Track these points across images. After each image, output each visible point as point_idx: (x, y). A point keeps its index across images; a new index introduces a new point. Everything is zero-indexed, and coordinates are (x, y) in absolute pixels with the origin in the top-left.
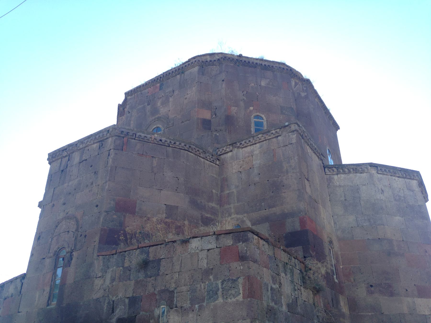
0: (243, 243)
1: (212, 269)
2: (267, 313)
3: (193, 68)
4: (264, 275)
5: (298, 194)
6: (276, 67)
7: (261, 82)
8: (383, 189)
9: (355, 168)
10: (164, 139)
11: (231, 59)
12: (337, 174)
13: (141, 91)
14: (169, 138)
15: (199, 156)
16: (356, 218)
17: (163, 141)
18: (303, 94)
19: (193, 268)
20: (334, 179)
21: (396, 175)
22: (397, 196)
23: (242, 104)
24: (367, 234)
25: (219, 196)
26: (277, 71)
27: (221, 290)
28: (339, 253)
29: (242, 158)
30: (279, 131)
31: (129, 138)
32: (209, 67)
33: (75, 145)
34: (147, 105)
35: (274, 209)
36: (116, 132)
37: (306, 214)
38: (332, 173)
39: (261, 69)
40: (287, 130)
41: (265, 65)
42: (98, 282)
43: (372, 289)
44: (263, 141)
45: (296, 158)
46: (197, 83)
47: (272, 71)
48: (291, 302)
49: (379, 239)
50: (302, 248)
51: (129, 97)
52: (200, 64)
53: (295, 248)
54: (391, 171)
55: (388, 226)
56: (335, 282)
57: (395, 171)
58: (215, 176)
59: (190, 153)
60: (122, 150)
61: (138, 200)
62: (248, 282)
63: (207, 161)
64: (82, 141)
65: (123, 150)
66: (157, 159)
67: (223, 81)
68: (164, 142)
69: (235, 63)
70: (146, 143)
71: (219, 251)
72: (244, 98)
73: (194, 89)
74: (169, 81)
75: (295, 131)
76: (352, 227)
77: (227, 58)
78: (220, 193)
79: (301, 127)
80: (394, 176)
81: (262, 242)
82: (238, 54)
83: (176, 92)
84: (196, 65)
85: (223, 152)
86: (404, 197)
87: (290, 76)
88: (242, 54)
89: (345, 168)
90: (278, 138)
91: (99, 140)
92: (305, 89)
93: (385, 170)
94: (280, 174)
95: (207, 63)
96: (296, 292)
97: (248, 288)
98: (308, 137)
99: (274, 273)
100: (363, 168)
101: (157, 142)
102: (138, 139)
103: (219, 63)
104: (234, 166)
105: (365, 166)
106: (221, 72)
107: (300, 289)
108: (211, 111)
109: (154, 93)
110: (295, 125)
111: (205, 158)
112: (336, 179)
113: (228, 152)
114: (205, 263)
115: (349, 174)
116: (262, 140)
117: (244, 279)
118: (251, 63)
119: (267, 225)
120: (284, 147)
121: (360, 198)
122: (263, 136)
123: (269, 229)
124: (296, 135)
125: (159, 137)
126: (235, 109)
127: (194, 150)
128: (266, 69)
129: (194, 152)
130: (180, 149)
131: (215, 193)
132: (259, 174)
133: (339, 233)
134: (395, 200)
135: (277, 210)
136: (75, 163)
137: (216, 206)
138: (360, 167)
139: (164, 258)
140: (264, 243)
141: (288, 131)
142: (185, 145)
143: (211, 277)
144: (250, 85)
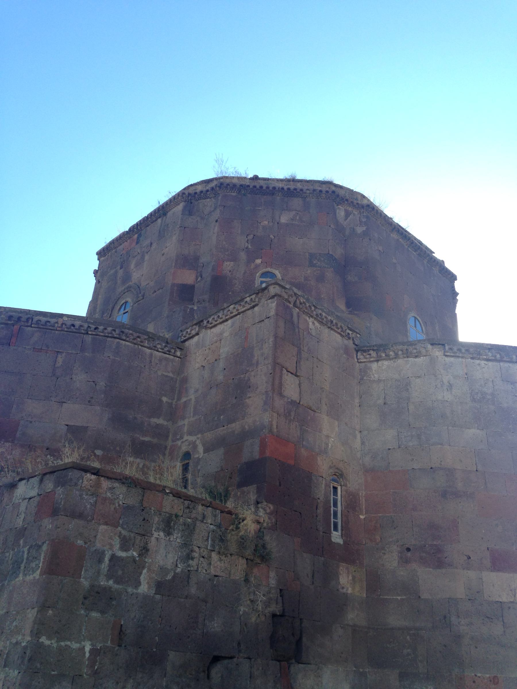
0: (61, 488)
2: (85, 598)
3: (177, 205)
4: (98, 537)
6: (307, 190)
7: (280, 217)
9: (405, 348)
12: (377, 361)
13: (115, 248)
15: (142, 346)
16: (397, 434)
17: (77, 327)
18: (360, 230)
20: (372, 369)
21: (481, 357)
22: (478, 393)
23: (243, 256)
26: (309, 196)
27: (25, 561)
35: (233, 425)
38: (368, 360)
40: (266, 295)
41: (289, 189)
43: (409, 554)
44: (236, 315)
45: (272, 339)
47: (302, 198)
48: (169, 577)
49: (431, 468)
50: (256, 488)
52: (187, 198)
54: (471, 350)
56: (330, 543)
57: (479, 350)
58: (171, 375)
59: (124, 342)
60: (9, 345)
63: (157, 353)
66: (64, 354)
69: (239, 192)
72: (248, 246)
77: (225, 185)
78: (176, 402)
80: (478, 360)
81: (105, 484)
83: (154, 246)
84: (180, 200)
85: (188, 336)
87: (335, 201)
88: (257, 175)
89: (390, 349)
90: (255, 308)
92: (364, 220)
94: (248, 369)
95: (196, 196)
96: (191, 562)
98: (307, 304)
100: (418, 348)
101: (67, 328)
103: (214, 194)
104: (198, 357)
105: (423, 345)
106: (215, 208)
107: (206, 556)
109: (130, 249)
110: (275, 286)
111: (153, 348)
115: (396, 360)
116: (234, 314)
120: (260, 323)
121: (408, 399)
124: (276, 303)
125: (70, 321)
126: (230, 265)
127: (132, 337)
128: (291, 194)
131: (166, 402)
132: (225, 369)
134: (474, 400)
135: (236, 426)
137: (165, 423)
138: (413, 347)
140: (116, 485)
141: (267, 296)
142: (115, 330)
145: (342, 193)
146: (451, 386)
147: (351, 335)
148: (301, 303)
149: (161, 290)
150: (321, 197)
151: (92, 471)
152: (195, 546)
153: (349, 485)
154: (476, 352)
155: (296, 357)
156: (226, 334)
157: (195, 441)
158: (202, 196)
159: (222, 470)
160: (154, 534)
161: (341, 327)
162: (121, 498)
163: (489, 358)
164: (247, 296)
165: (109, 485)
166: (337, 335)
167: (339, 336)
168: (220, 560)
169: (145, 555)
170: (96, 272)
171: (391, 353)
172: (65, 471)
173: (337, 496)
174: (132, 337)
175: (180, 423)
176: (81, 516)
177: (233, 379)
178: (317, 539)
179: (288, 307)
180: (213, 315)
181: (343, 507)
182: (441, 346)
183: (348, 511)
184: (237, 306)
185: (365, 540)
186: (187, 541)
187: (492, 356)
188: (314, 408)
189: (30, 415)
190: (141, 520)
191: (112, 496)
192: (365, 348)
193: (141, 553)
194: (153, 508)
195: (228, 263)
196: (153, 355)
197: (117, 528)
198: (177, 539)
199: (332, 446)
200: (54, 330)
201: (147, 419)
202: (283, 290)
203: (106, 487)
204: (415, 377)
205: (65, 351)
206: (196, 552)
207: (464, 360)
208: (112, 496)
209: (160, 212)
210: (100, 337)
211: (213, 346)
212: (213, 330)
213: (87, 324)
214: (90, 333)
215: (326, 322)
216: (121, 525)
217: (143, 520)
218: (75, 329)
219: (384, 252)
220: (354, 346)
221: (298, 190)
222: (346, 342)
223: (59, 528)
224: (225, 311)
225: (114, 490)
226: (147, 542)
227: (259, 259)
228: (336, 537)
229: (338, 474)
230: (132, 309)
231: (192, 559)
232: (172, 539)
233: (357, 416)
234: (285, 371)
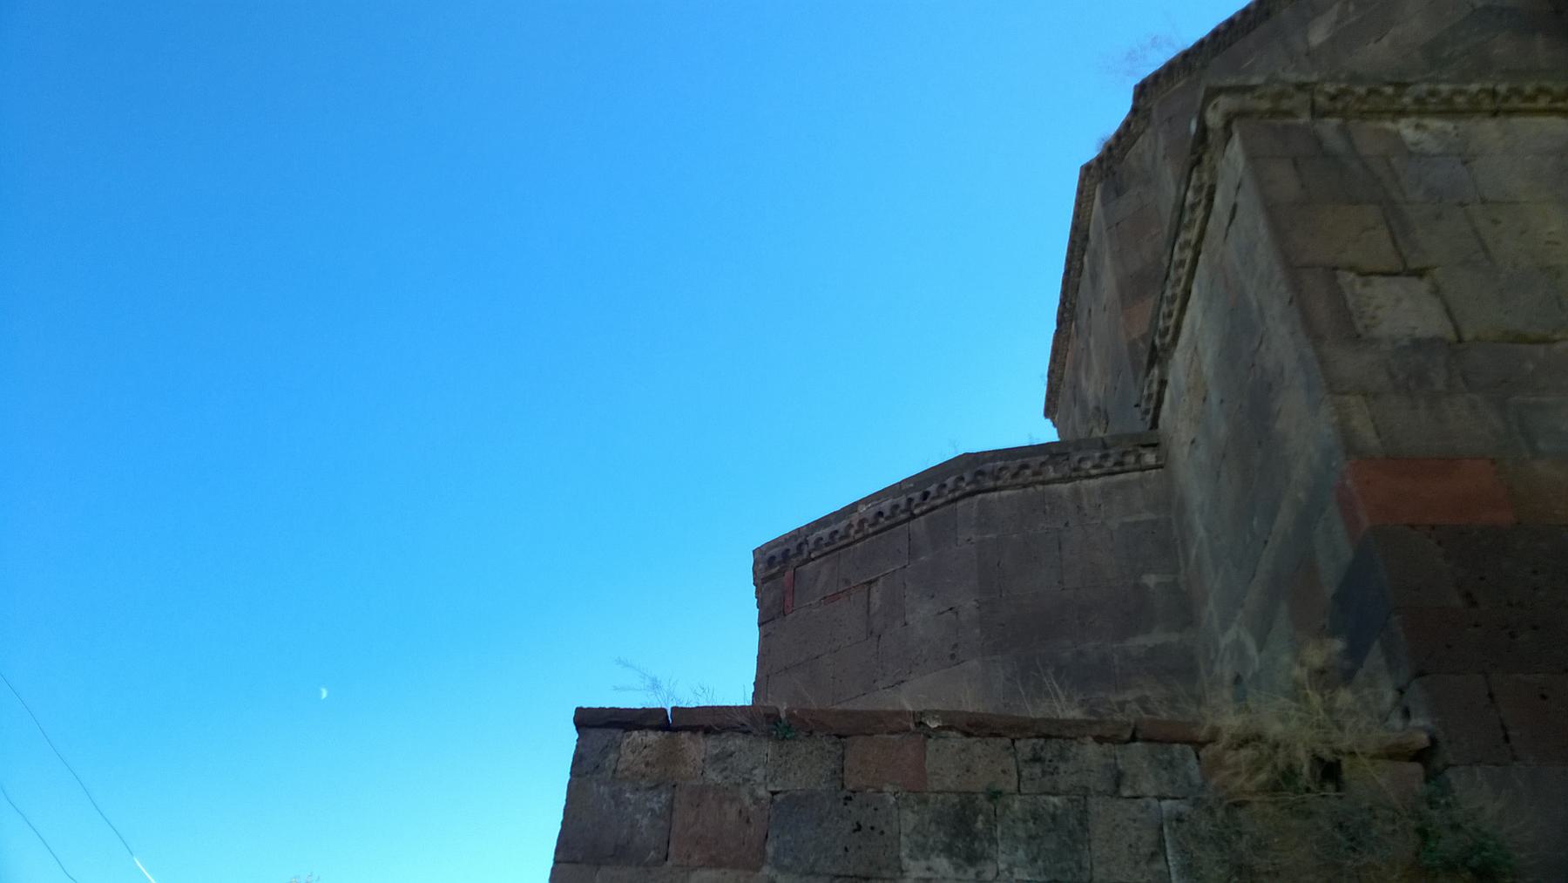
15: (1043, 483)
31: (797, 567)
58: (1147, 516)
59: (996, 495)
63: (1091, 481)
111: (1074, 474)
125: (872, 509)
137: (1174, 638)
140: (736, 743)
142: (962, 479)
148: (1333, 98)
162: (759, 779)
165: (709, 749)
174: (1007, 475)
194: (888, 788)
197: (758, 869)
198: (1016, 870)
201: (1115, 646)
203: (703, 757)
208: (726, 778)
214: (916, 511)
217: (855, 831)
225: (730, 760)
234: (1347, 278)
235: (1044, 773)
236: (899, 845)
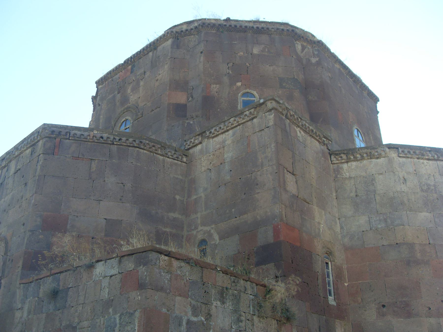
0: (143, 267)
1: (113, 300)
3: (166, 41)
4: (176, 306)
5: (273, 194)
6: (272, 28)
8: (405, 178)
9: (369, 152)
10: (105, 135)
11: (211, 25)
12: (347, 162)
13: (112, 78)
14: (112, 134)
15: (156, 153)
16: (368, 219)
17: (105, 138)
18: (314, 60)
19: (96, 300)
20: (343, 169)
21: (424, 157)
23: (226, 80)
24: (382, 238)
25: (185, 203)
26: (274, 33)
27: (118, 325)
28: (345, 266)
29: (213, 152)
30: (254, 112)
31: (62, 139)
32: (185, 37)
33: (11, 152)
34: (117, 94)
35: (245, 216)
36: (46, 133)
37: (282, 220)
38: (340, 161)
39: (253, 33)
40: (263, 109)
41: (258, 28)
42: (18, 314)
44: (236, 126)
45: (273, 145)
46: (170, 59)
47: (268, 35)
49: (397, 244)
51: (101, 86)
53: (266, 265)
54: (417, 152)
55: (409, 226)
56: (328, 305)
58: (180, 177)
59: (142, 151)
60: (53, 154)
61: (71, 215)
62: (144, 316)
63: (168, 159)
64: (17, 147)
65: (54, 154)
66: (96, 161)
67: (202, 53)
68: (105, 139)
70: (84, 142)
71: (121, 278)
72: (229, 72)
73: (166, 67)
74: (141, 61)
75: (272, 109)
76: (363, 231)
78: (186, 200)
79: (283, 104)
80: (422, 159)
81: (176, 263)
82: (225, 18)
83: (148, 74)
85: (191, 145)
86: (435, 186)
89: (357, 153)
90: (254, 120)
91: (31, 144)
92: (316, 53)
93: (409, 152)
94: (253, 170)
95: (182, 33)
96: (240, 324)
97: (143, 324)
98: (295, 116)
99: (197, 302)
100: (379, 151)
101: (97, 140)
102: (73, 138)
103: (197, 32)
105: (382, 149)
106: (199, 43)
107: (250, 319)
108: (187, 93)
109: (125, 77)
112: (345, 169)
113: (197, 145)
114: (106, 293)
115: (362, 161)
116: (235, 125)
117: (140, 312)
118: (238, 27)
119: (236, 238)
120: (260, 132)
121: (375, 191)
122: (235, 120)
123: (238, 243)
124: (274, 115)
127: (148, 146)
128: (260, 32)
129: (148, 149)
130: (127, 146)
131: (179, 199)
132: (231, 171)
133: (346, 240)
134: (422, 190)
135: (248, 217)
136: (11, 174)
137: (180, 217)
138: (375, 150)
139: (72, 287)
140: (183, 264)
141: (265, 110)
142: (135, 141)
143: (111, 310)
144: (238, 54)
145: (298, 31)
146: (406, 181)
147: (325, 142)
148: (291, 116)
149: (158, 109)
150: (283, 34)
151: (165, 253)
152: (242, 311)
153: (336, 261)
154: (420, 154)
155: (292, 159)
156: (229, 142)
157: (210, 231)
158: (187, 34)
159: (239, 253)
160: (213, 303)
161: (319, 134)
163: (430, 158)
164: (246, 110)
166: (316, 141)
167: (317, 142)
168: (260, 321)
169: (209, 319)
170: (94, 99)
171: (358, 156)
172: (144, 253)
173: (329, 269)
174: (148, 146)
175: (193, 216)
176: (161, 289)
177: (240, 179)
178: (320, 303)
179: (282, 118)
180: (214, 126)
181: (334, 278)
182: (396, 149)
183: (337, 281)
184: (237, 119)
185: (349, 302)
186: (236, 308)
187: (432, 156)
188: (308, 201)
189: (76, 211)
190: (204, 292)
191: (181, 273)
192: (337, 152)
193: (206, 318)
195: (215, 86)
196: (165, 161)
197: (188, 298)
199: (322, 231)
200: (87, 141)
201: (166, 214)
202: (278, 105)
203: (176, 266)
204: (378, 174)
205: (97, 159)
206: (243, 316)
207: (412, 160)
208: (181, 273)
209: (151, 47)
210: (123, 147)
211: (217, 152)
212: (215, 139)
213: (112, 136)
215: (309, 131)
216: (191, 296)
217: (205, 292)
218: (104, 140)
219: (332, 78)
220: (327, 151)
221: (265, 29)
222: (322, 147)
223: (148, 299)
224: (226, 123)
225: (182, 269)
226: (209, 309)
227: (239, 82)
228: (331, 300)
229: (328, 253)
230: (133, 125)
231: (241, 321)
232: (226, 307)
233: (336, 207)
235: (235, 285)
236: (212, 297)
